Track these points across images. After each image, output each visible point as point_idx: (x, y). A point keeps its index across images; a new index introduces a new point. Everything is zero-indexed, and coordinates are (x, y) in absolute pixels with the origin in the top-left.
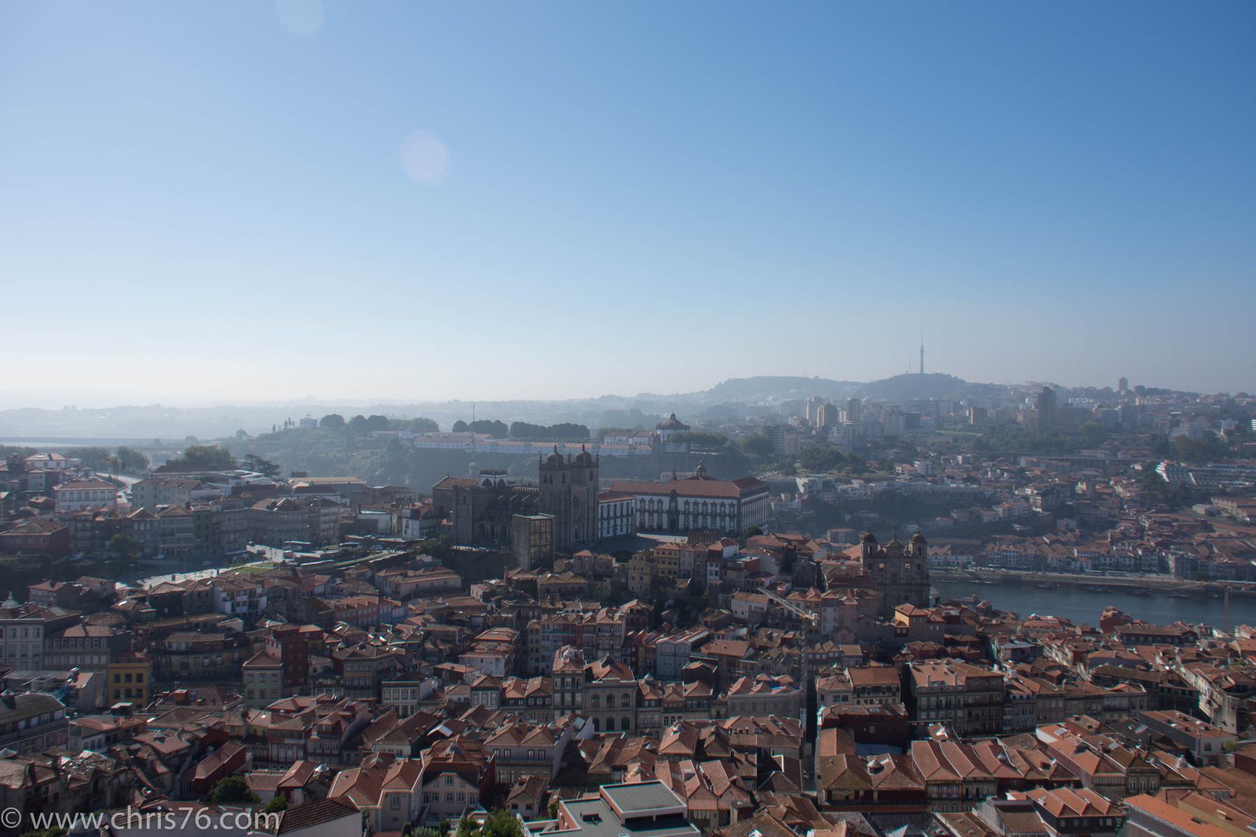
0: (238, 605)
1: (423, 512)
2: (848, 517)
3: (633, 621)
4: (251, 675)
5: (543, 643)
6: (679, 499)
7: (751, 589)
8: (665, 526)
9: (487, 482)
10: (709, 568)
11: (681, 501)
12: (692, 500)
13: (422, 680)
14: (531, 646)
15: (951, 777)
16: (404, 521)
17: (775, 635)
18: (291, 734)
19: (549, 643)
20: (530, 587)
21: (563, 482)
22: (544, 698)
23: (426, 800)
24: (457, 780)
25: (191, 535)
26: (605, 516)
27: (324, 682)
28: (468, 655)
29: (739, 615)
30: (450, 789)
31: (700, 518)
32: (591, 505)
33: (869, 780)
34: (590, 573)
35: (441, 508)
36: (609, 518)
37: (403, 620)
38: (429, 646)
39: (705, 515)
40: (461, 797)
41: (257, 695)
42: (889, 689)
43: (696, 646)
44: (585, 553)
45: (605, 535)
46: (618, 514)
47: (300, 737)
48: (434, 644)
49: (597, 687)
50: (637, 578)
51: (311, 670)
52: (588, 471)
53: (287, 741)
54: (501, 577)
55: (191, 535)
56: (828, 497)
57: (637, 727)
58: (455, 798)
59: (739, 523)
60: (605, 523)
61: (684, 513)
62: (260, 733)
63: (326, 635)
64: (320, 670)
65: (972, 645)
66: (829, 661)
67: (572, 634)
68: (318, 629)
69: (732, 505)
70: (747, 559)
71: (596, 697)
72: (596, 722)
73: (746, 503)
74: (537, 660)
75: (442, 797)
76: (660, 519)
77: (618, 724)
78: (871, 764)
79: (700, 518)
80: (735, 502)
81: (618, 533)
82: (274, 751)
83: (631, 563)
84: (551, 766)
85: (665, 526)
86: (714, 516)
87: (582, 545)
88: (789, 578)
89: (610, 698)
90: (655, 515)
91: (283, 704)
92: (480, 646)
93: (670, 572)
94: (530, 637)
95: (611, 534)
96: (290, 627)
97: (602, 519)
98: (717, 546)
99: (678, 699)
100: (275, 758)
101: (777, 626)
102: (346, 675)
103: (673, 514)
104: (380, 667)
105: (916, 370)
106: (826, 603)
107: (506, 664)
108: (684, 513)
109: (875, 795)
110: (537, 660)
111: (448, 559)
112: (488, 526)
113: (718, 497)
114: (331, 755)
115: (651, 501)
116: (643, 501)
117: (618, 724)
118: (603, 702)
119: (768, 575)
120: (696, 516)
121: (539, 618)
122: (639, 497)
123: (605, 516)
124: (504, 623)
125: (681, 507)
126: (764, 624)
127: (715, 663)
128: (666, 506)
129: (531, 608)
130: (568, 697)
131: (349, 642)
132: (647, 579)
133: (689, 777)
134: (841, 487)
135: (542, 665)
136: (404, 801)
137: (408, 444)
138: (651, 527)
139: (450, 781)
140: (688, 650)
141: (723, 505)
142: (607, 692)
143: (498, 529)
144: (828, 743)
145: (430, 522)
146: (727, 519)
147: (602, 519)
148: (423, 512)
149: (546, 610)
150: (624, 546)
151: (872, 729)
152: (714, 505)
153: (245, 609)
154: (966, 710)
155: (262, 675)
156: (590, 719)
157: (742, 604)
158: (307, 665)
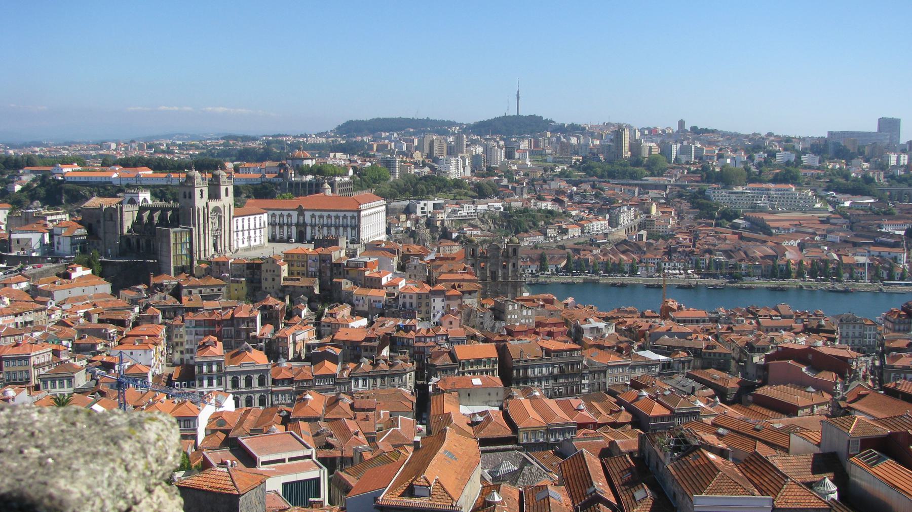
11: (308, 215)
12: (317, 214)
14: (175, 340)
26: (240, 228)
29: (361, 308)
31: (325, 229)
39: (329, 227)
45: (241, 245)
46: (252, 227)
50: (270, 279)
54: (147, 282)
60: (240, 234)
69: (353, 217)
80: (356, 214)
81: (253, 243)
86: (337, 227)
90: (285, 228)
95: (246, 244)
97: (237, 231)
105: (513, 113)
108: (311, 225)
110: (182, 352)
115: (281, 216)
116: (274, 215)
118: (242, 382)
122: (271, 212)
125: (308, 220)
128: (294, 220)
138: (282, 238)
141: (345, 217)
143: (143, 242)
146: (349, 229)
152: (337, 217)
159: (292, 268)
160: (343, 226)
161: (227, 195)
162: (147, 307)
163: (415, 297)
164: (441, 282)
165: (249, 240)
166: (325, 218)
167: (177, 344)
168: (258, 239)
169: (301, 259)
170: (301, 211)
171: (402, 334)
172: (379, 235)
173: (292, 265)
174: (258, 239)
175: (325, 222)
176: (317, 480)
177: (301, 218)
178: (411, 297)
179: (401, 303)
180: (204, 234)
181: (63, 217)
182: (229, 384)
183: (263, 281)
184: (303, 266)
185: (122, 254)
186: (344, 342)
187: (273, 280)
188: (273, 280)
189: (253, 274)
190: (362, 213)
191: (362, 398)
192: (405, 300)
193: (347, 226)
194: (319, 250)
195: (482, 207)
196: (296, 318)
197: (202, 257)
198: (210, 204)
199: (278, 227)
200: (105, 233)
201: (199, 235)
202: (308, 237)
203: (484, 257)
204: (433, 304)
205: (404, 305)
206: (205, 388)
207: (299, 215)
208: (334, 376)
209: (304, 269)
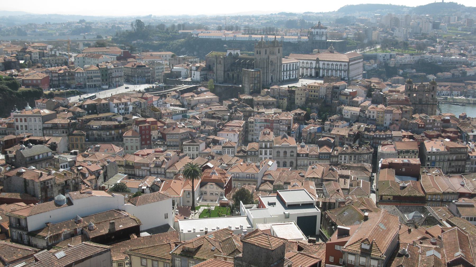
0: (120, 109)
2: (401, 72)
3: (297, 119)
4: (127, 140)
5: (256, 128)
6: (320, 62)
8: (313, 75)
9: (230, 54)
11: (321, 63)
12: (326, 63)
15: (438, 192)
16: (193, 72)
17: (362, 126)
18: (144, 165)
21: (266, 54)
22: (255, 152)
24: (215, 186)
25: (100, 79)
26: (285, 69)
27: (158, 143)
29: (346, 117)
31: (330, 71)
32: (279, 64)
34: (278, 96)
35: (210, 66)
39: (332, 70)
41: (129, 148)
42: (413, 152)
45: (285, 78)
46: (291, 69)
50: (299, 99)
51: (152, 138)
52: (278, 48)
53: (142, 168)
55: (100, 79)
56: (392, 63)
57: (297, 165)
59: (348, 74)
61: (322, 69)
62: (131, 164)
64: (156, 138)
65: (455, 133)
69: (345, 65)
71: (278, 152)
72: (278, 163)
75: (208, 193)
76: (311, 71)
77: (288, 164)
79: (330, 71)
81: (291, 78)
82: (137, 172)
84: (257, 181)
85: (313, 75)
86: (336, 71)
89: (285, 152)
90: (309, 69)
92: (227, 128)
93: (314, 96)
94: (250, 124)
99: (315, 153)
100: (138, 175)
101: (364, 122)
102: (167, 140)
103: (317, 70)
104: (182, 137)
106: (387, 112)
108: (322, 69)
112: (231, 75)
114: (160, 174)
115: (307, 63)
117: (288, 164)
118: (282, 154)
120: (328, 70)
125: (321, 66)
126: (357, 121)
128: (314, 66)
132: (304, 99)
134: (399, 57)
138: (307, 75)
141: (341, 65)
142: (284, 150)
143: (235, 75)
146: (343, 72)
151: (404, 170)
152: (337, 65)
153: (123, 111)
154: (449, 162)
155: (131, 140)
158: (150, 136)
159: (311, 93)
160: (339, 70)
161: (279, 53)
162: (236, 111)
163: (375, 112)
164: (389, 104)
165: (290, 77)
166: (330, 65)
168: (294, 76)
169: (316, 89)
171: (366, 133)
172: (359, 75)
173: (312, 92)
174: (294, 76)
175: (330, 68)
176: (315, 217)
177: (317, 65)
178: (374, 113)
179: (368, 116)
180: (267, 73)
181: (197, 59)
182: (276, 154)
183: (296, 100)
184: (317, 92)
185: (225, 82)
187: (301, 99)
188: (301, 99)
189: (291, 95)
190: (350, 63)
191: (343, 169)
192: (370, 114)
193: (342, 70)
194: (326, 84)
195: (417, 58)
196: (312, 121)
197: (265, 84)
198: (270, 57)
199: (305, 69)
200: (217, 70)
201: (264, 73)
202: (321, 75)
204: (385, 117)
205: (370, 116)
206: (263, 156)
207: (316, 63)
208: (330, 154)
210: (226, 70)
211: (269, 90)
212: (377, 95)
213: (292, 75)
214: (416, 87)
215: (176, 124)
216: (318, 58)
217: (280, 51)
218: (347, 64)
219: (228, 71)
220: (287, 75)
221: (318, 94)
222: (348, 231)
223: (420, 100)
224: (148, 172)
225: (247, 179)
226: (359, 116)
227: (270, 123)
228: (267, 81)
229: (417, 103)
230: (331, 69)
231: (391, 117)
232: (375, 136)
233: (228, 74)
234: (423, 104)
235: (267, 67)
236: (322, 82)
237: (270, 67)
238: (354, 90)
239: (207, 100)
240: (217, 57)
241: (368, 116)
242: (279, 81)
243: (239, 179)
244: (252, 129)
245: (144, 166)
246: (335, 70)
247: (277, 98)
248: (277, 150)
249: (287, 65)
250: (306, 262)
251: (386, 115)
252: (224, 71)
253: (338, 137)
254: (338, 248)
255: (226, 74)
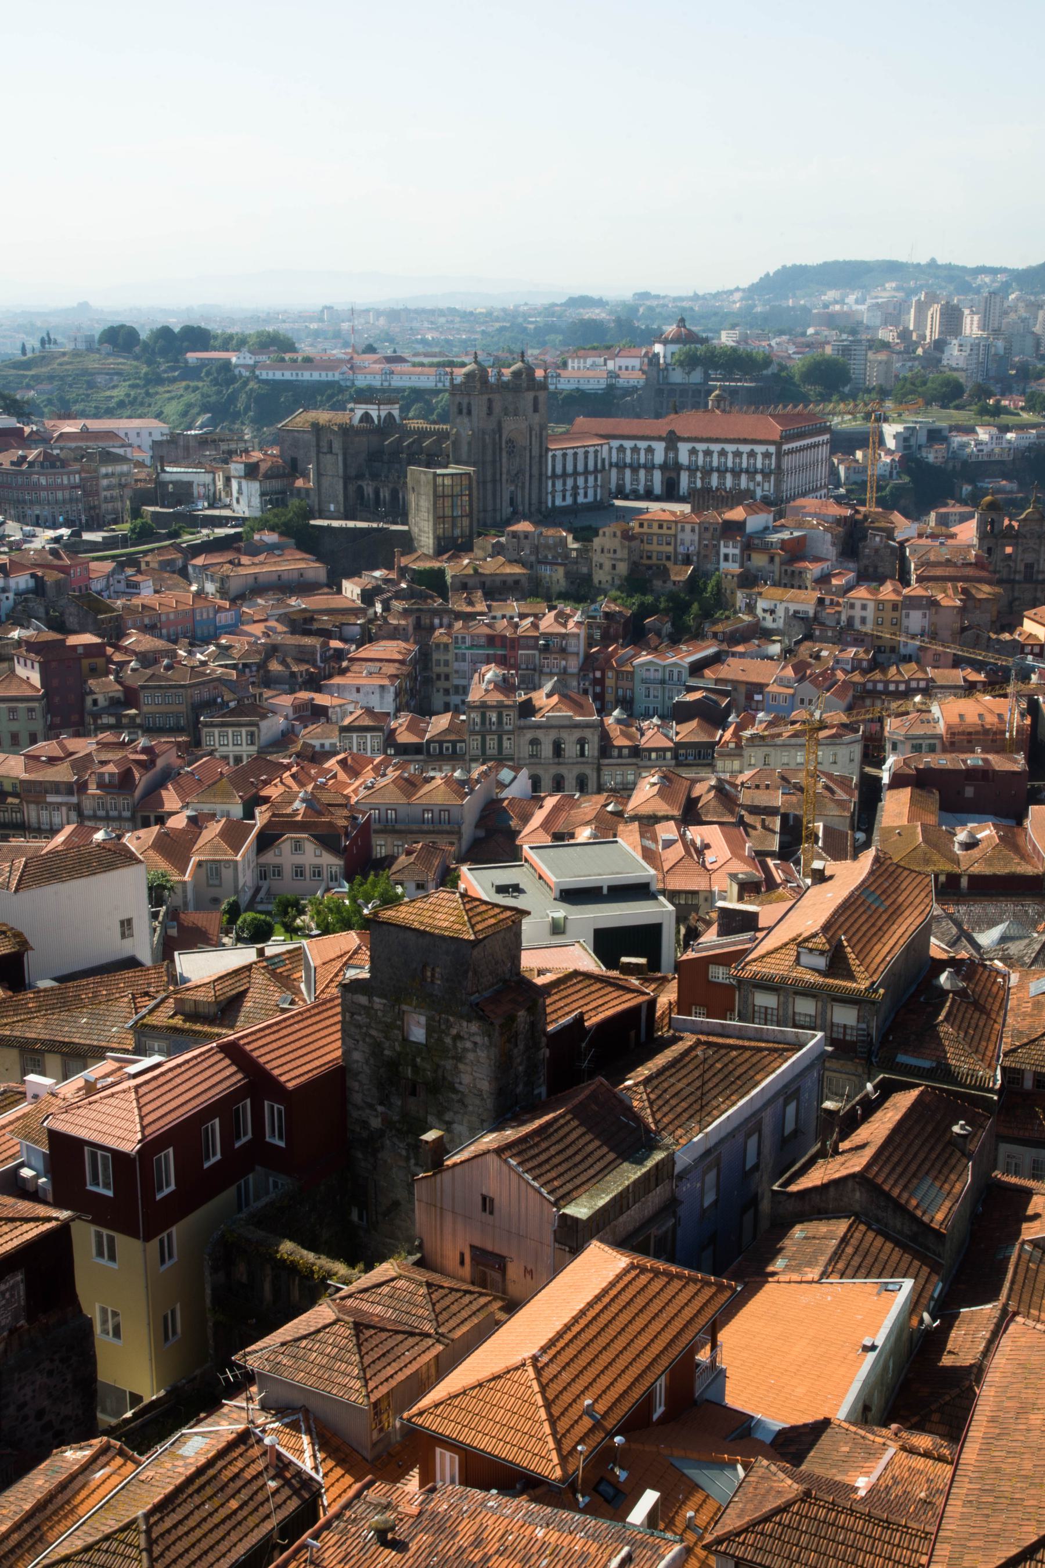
1: (263, 467)
2: (967, 489)
5: (456, 665)
7: (792, 580)
8: (658, 489)
9: (366, 417)
10: (723, 550)
11: (684, 448)
12: (701, 447)
13: (264, 717)
14: (437, 669)
17: (824, 653)
18: (56, 788)
19: (465, 666)
20: (434, 581)
21: (490, 413)
23: (263, 875)
26: (559, 470)
28: (337, 680)
30: (298, 859)
32: (535, 452)
33: (957, 861)
36: (564, 475)
37: (232, 629)
38: (275, 666)
39: (722, 471)
40: (317, 872)
43: (697, 668)
44: (524, 526)
45: (559, 502)
46: (580, 468)
47: (70, 792)
48: (283, 662)
49: (538, 726)
50: (607, 565)
51: (89, 700)
52: (530, 396)
53: (51, 799)
54: (389, 567)
58: (308, 873)
61: (688, 468)
63: (109, 650)
64: (102, 702)
66: (908, 694)
67: (501, 648)
68: (97, 640)
69: (767, 455)
70: (785, 535)
71: (535, 742)
73: (791, 452)
74: (447, 692)
75: (288, 872)
76: (650, 479)
77: (570, 781)
78: (962, 836)
80: (772, 449)
81: (581, 499)
82: (31, 814)
83: (597, 542)
84: (459, 833)
85: (658, 489)
86: (736, 473)
87: (516, 516)
88: (851, 565)
90: (642, 473)
91: (45, 748)
94: (435, 656)
95: (569, 501)
96: (52, 636)
97: (554, 476)
98: (737, 514)
102: (145, 709)
103: (671, 469)
104: (197, 698)
106: (912, 603)
107: (397, 695)
109: (964, 882)
110: (447, 692)
111: (307, 540)
112: (369, 490)
113: (745, 441)
114: (120, 818)
115: (635, 450)
116: (621, 449)
117: (570, 781)
119: (817, 559)
120: (707, 472)
121: (450, 626)
122: (615, 444)
123: (559, 470)
124: (395, 634)
125: (684, 458)
126: (808, 637)
127: (725, 694)
128: (659, 458)
129: (436, 612)
130: (492, 742)
131: (147, 659)
132: (623, 568)
133: (668, 844)
134: (958, 439)
135: (455, 699)
136: (227, 873)
137: (246, 373)
139: (298, 847)
140: (685, 673)
141: (752, 454)
142: (553, 735)
143: (385, 494)
144: (895, 808)
145: (276, 484)
147: (554, 476)
148: (263, 467)
149: (459, 616)
150: (584, 520)
152: (738, 454)
156: (524, 773)
157: (775, 605)
159: (648, 547)
160: (747, 471)
165: (575, 495)
167: (439, 677)
168: (590, 492)
169: (665, 531)
170: (672, 440)
174: (590, 492)
178: (864, 607)
179: (844, 618)
180: (494, 481)
184: (669, 544)
186: (735, 683)
187: (614, 567)
188: (614, 567)
190: (785, 447)
192: (851, 612)
198: (504, 425)
199: (628, 472)
201: (484, 483)
203: (1009, 535)
204: (905, 622)
205: (850, 620)
207: (667, 449)
209: (670, 549)
210: (353, 472)
211: (503, 539)
212: (877, 551)
213: (581, 492)
214: (1015, 524)
215: (173, 654)
216: (672, 433)
217: (541, 406)
218: (772, 449)
219: (360, 476)
220: (564, 491)
221: (670, 549)
222: (755, 916)
223: (1029, 566)
224: (73, 815)
225: (425, 827)
226: (816, 618)
227: (503, 646)
228: (494, 510)
229: (1017, 577)
230: (718, 470)
231: (926, 623)
232: (870, 686)
233: (360, 488)
234: (1037, 582)
235: (494, 462)
236: (687, 508)
237: (504, 460)
238: (796, 534)
239: (285, 577)
240: (317, 428)
241: (844, 618)
242: (539, 511)
243: (398, 827)
244: (446, 670)
245: (57, 792)
246: (733, 471)
247: (531, 567)
248: (529, 735)
249: (565, 455)
250: (600, 1002)
251: (907, 616)
252: (347, 479)
253: (742, 689)
254: (719, 974)
255: (351, 488)
